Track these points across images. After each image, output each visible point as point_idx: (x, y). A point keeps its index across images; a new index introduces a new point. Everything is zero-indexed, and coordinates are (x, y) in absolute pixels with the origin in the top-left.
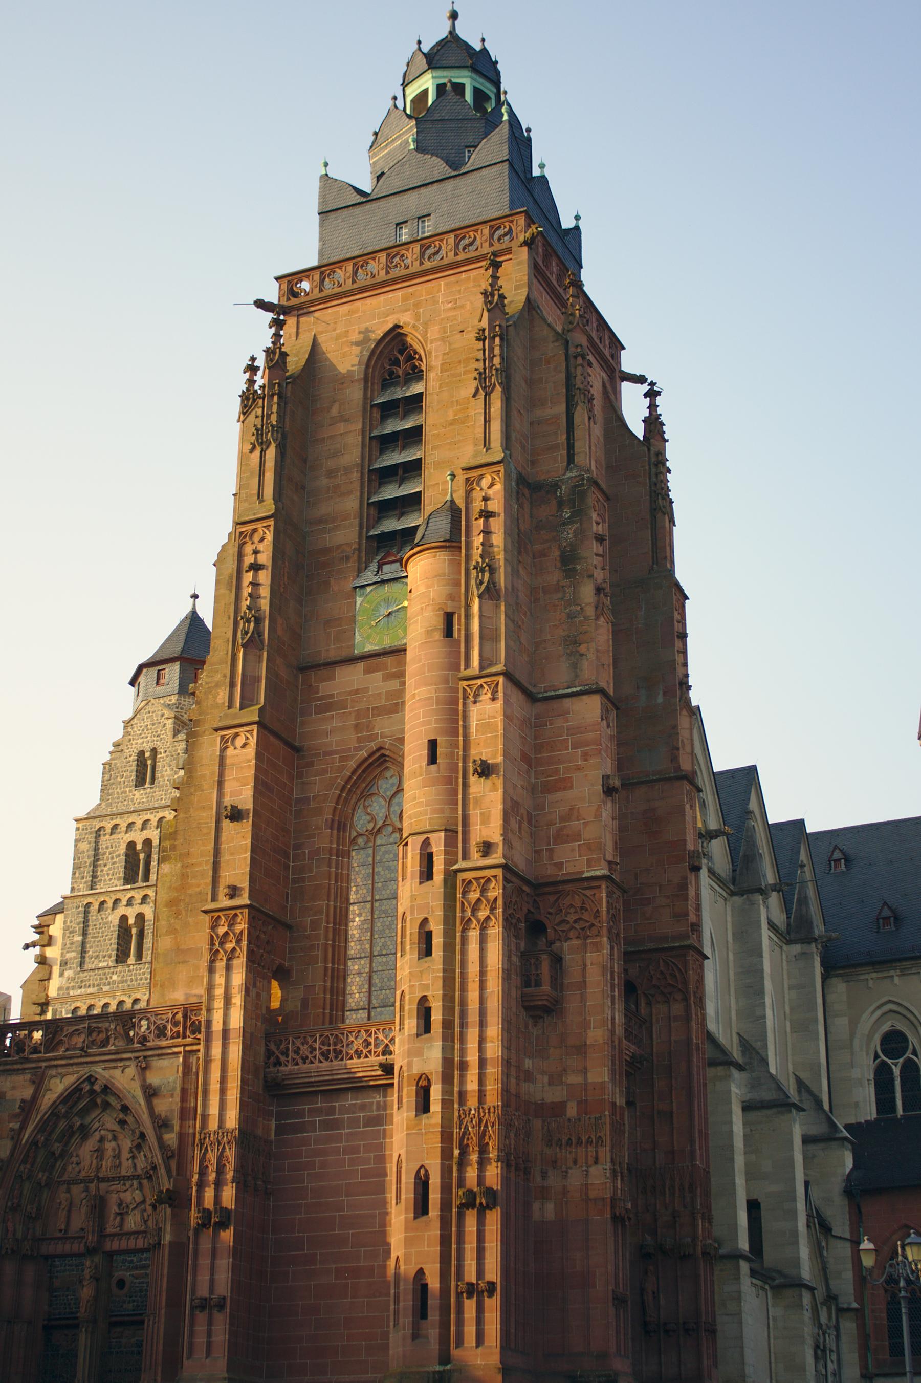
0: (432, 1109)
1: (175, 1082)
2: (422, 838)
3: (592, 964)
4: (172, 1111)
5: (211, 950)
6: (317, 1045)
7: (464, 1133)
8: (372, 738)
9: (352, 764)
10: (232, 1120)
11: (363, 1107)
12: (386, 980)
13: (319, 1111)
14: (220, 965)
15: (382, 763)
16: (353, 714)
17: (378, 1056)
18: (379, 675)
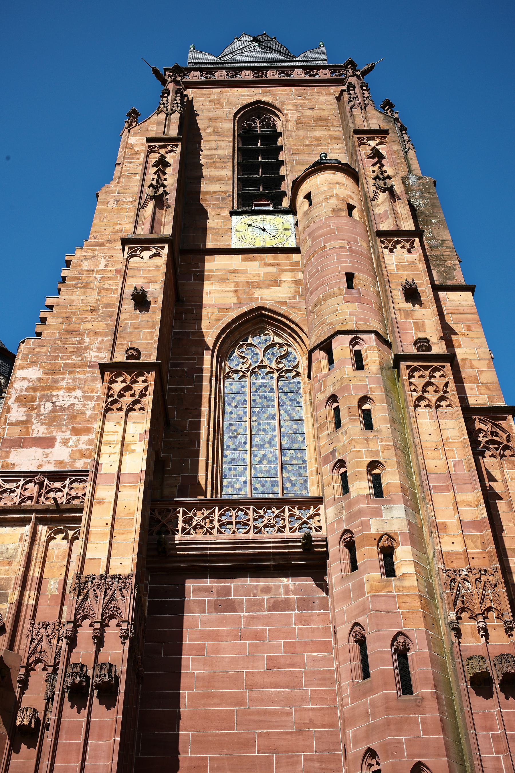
0: (399, 572)
1: (16, 550)
2: (352, 336)
3: (512, 479)
4: (8, 579)
5: (107, 400)
6: (216, 516)
7: (457, 597)
8: (253, 299)
9: (233, 315)
10: (125, 563)
11: (267, 590)
12: (268, 485)
13: (210, 590)
14: (115, 416)
15: (257, 324)
16: (232, 285)
17: (294, 531)
18: (257, 263)
